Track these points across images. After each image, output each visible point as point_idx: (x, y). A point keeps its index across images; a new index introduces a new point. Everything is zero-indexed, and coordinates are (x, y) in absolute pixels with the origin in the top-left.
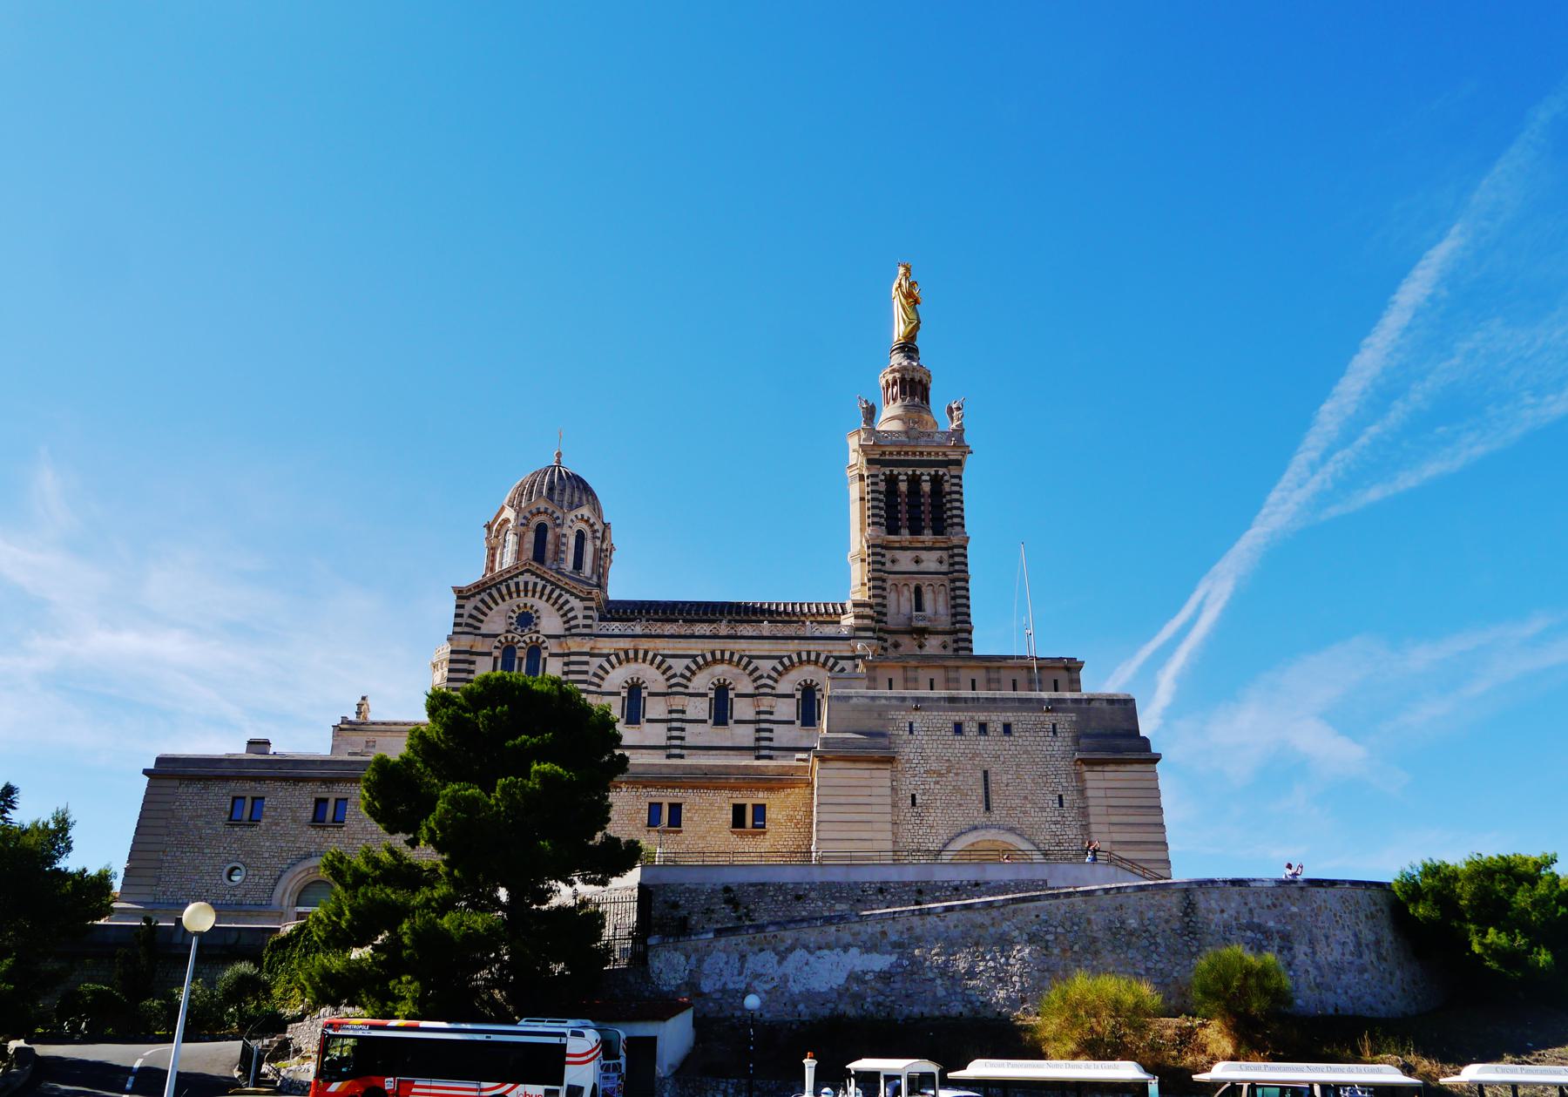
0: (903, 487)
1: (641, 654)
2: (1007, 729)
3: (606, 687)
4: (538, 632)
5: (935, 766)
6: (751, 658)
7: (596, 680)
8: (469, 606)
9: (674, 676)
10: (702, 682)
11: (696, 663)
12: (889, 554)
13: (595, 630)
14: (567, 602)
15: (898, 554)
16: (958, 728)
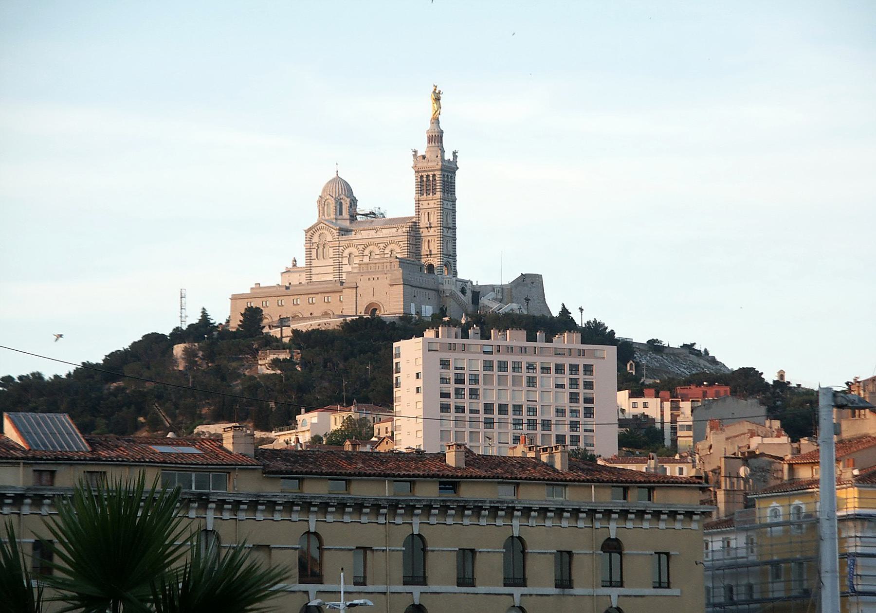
0: (425, 179)
1: (351, 245)
2: (378, 278)
3: (344, 255)
4: (326, 241)
5: (364, 288)
6: (378, 243)
7: (341, 253)
8: (309, 233)
9: (360, 251)
10: (367, 252)
11: (365, 246)
12: (421, 202)
13: (340, 239)
14: (332, 231)
15: (423, 202)
16: (369, 279)
